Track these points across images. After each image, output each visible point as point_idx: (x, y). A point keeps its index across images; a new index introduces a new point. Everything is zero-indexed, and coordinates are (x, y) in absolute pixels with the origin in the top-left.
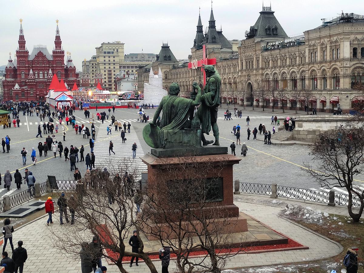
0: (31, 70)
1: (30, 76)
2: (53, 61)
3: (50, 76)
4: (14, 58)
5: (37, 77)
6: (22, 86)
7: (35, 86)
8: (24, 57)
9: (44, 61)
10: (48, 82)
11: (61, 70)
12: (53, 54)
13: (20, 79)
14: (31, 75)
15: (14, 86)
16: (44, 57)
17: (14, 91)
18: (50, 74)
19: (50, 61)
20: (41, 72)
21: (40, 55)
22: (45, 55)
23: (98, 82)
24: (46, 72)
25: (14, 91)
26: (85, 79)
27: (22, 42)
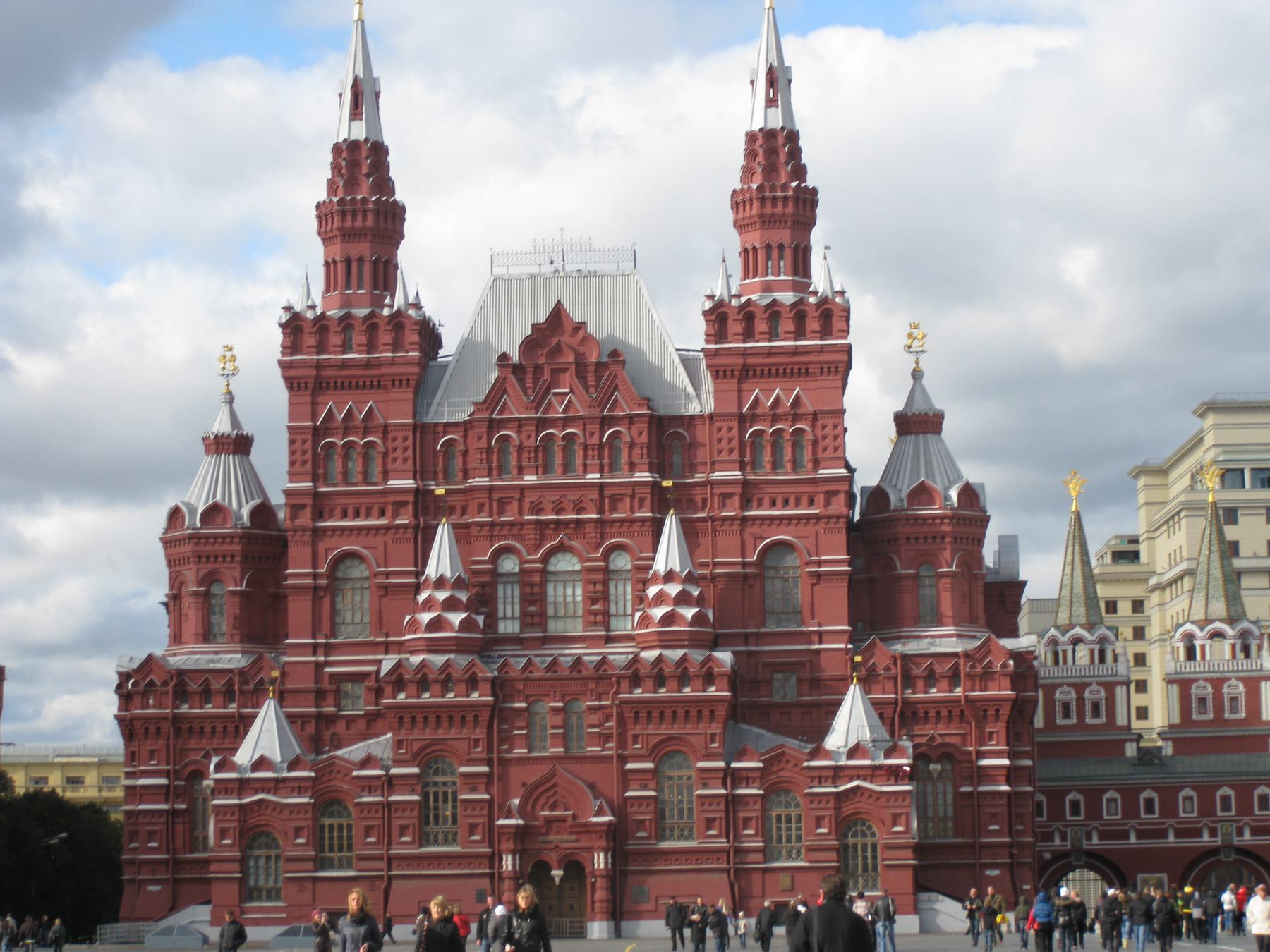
0: (443, 538)
1: (428, 605)
2: (711, 416)
4: (269, 408)
5: (508, 627)
6: (340, 727)
7: (480, 733)
8: (376, 384)
9: (606, 422)
10: (636, 680)
11: (802, 529)
12: (709, 337)
13: (315, 649)
14: (442, 595)
15: (240, 727)
16: (606, 368)
19: (680, 418)
20: (567, 563)
22: (615, 354)
23: (1219, 709)
25: (223, 788)
26: (1080, 688)
27: (364, 211)
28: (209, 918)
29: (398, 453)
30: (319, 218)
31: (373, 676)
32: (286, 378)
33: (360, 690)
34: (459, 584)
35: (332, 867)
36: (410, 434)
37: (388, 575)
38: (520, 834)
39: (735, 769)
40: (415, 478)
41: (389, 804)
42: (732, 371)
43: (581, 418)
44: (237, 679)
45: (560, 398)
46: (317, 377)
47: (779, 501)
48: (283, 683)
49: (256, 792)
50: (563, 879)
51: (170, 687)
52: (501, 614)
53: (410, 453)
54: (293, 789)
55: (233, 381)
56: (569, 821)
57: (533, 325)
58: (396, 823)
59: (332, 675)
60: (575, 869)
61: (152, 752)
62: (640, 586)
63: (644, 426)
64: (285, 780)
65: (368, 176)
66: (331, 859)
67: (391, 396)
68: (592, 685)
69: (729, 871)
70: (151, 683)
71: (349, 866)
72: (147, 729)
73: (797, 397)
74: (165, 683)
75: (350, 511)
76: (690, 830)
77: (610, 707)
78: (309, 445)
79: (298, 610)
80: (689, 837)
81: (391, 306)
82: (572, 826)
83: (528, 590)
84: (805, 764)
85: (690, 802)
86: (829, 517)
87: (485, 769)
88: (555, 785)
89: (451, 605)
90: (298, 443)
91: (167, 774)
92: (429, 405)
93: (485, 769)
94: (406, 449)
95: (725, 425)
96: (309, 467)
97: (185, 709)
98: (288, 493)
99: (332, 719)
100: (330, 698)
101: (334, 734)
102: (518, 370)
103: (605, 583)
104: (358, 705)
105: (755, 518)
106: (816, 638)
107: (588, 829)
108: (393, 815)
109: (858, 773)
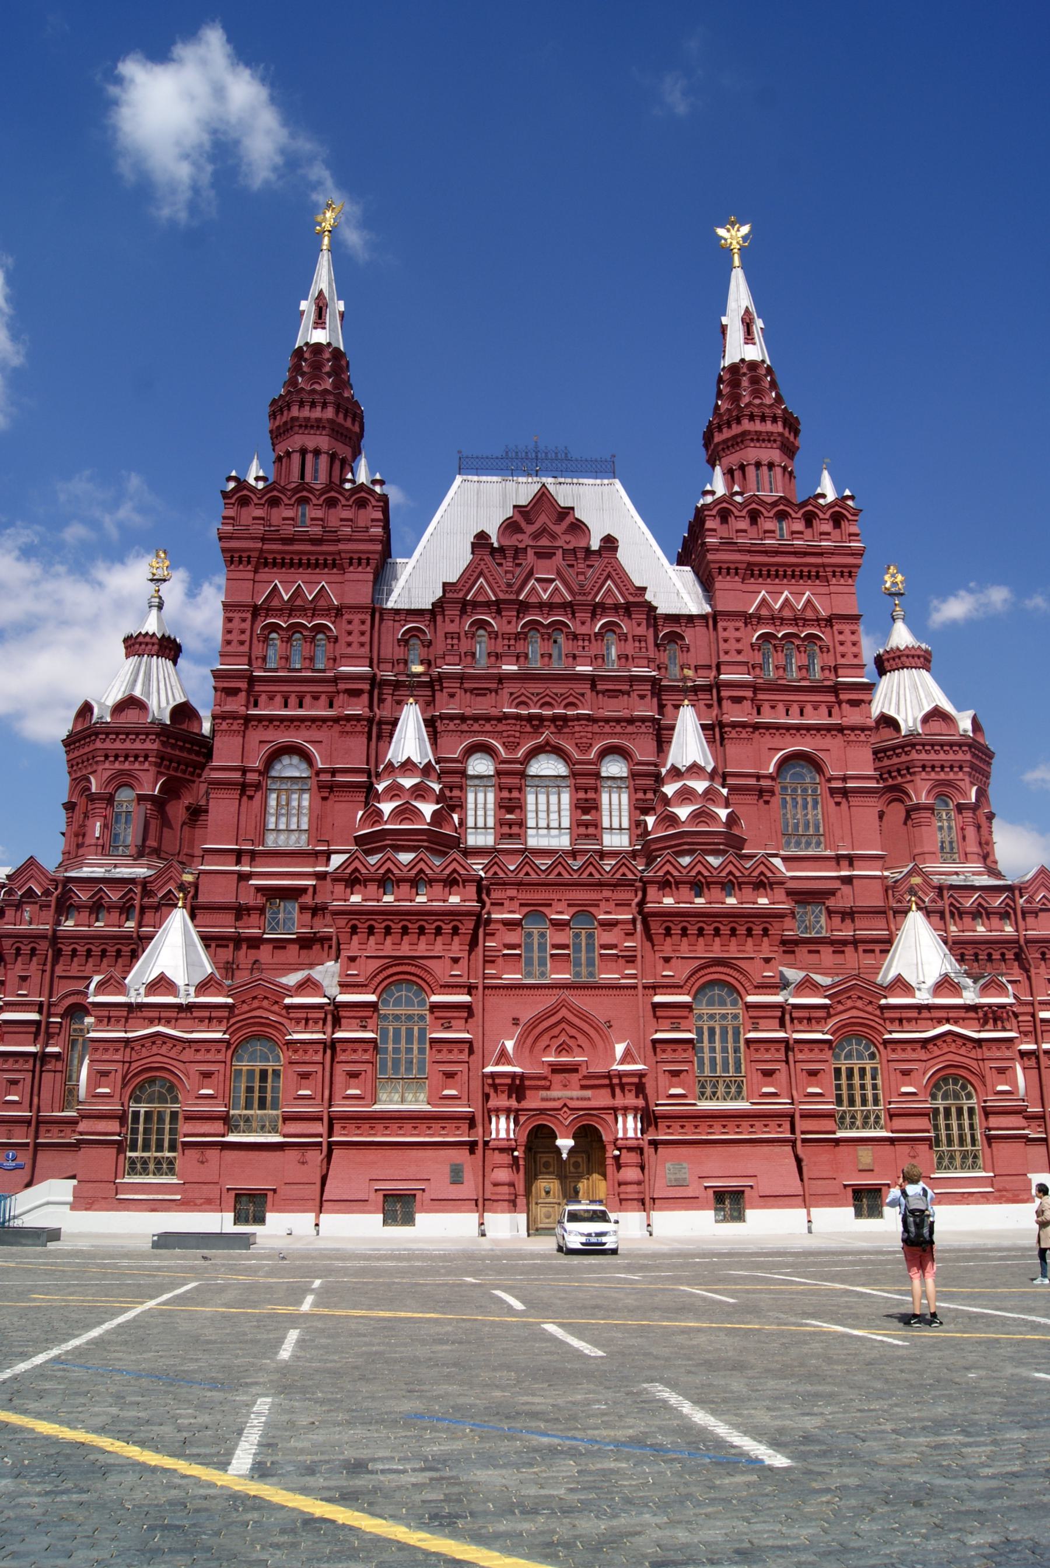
0: (411, 721)
1: (395, 791)
3: (686, 795)
6: (265, 954)
9: (597, 609)
13: (238, 856)
14: (408, 782)
15: (134, 947)
17: (108, 1014)
18: (695, 769)
19: (675, 619)
20: (547, 766)
21: (544, 542)
22: (610, 543)
24: (614, 768)
25: (108, 1014)
28: (71, 1199)
29: (354, 638)
30: (273, 416)
31: (311, 890)
32: (224, 550)
33: (294, 907)
34: (427, 770)
35: (250, 1130)
36: (368, 617)
37: (334, 772)
38: (517, 1086)
39: (795, 1006)
40: (371, 666)
41: (334, 1042)
42: (737, 569)
43: (570, 604)
44: (138, 890)
45: (545, 585)
46: (261, 550)
47: (795, 709)
48: (195, 896)
49: (151, 1021)
50: (572, 1151)
51: (53, 899)
52: (470, 822)
53: (366, 639)
54: (201, 1020)
55: (164, 587)
56: (583, 1071)
57: (515, 507)
58: (340, 1069)
59: (259, 889)
60: (589, 1138)
61: (24, 979)
62: (640, 795)
63: (640, 616)
64: (190, 1007)
65: (329, 375)
66: (247, 1119)
67: (348, 576)
68: (607, 893)
69: (793, 1142)
70: (30, 892)
71: (274, 1130)
72: (18, 949)
73: (809, 601)
74: (47, 893)
75: (293, 700)
76: (739, 1087)
77: (634, 921)
78: (247, 625)
79: (222, 809)
80: (738, 1096)
81: (353, 481)
82: (585, 1077)
83: (505, 794)
84: (883, 1001)
85: (736, 1050)
86: (853, 729)
87: (466, 998)
88: (563, 1020)
89: (420, 792)
90: (236, 624)
91: (40, 1008)
92: (389, 594)
93: (466, 998)
94: (363, 633)
95: (731, 625)
96: (245, 648)
97: (69, 925)
98: (217, 675)
99: (255, 943)
100: (254, 918)
101: (256, 962)
102: (493, 551)
103: (596, 790)
104: (291, 923)
105: (768, 727)
106: (845, 863)
107: (614, 1082)
108: (342, 1057)
109: (947, 1014)
